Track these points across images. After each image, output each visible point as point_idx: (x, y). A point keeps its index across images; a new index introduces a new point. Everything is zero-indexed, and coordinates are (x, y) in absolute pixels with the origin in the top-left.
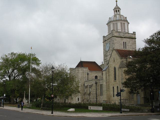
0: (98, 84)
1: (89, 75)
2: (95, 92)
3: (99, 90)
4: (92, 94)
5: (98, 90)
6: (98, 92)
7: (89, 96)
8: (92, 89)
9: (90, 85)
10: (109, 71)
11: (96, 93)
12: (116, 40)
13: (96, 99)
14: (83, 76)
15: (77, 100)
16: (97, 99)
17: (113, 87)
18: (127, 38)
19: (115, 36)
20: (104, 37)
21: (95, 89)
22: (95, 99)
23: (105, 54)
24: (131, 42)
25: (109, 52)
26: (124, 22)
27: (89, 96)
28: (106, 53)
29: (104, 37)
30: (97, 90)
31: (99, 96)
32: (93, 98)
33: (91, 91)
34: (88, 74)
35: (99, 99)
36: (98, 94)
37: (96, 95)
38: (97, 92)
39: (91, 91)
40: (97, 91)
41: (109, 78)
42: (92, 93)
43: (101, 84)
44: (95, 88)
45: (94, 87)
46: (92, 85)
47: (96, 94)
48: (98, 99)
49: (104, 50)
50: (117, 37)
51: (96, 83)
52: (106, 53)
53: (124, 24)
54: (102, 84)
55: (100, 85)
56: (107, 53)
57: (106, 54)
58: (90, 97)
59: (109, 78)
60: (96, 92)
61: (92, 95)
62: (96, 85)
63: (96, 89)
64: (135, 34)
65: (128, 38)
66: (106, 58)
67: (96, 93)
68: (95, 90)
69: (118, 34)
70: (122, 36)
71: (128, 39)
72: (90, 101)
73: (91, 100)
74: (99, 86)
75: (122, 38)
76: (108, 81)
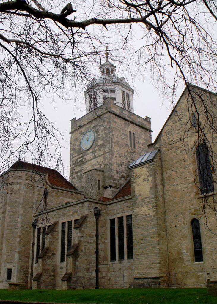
0: (102, 218)
1: (49, 197)
2: (93, 247)
3: (106, 241)
4: (85, 254)
5: (103, 240)
6: (101, 246)
7: (75, 261)
8: (84, 235)
9: (66, 220)
10: (162, 167)
11: (97, 248)
12: (115, 122)
13: (97, 271)
14: (33, 198)
15: (6, 276)
16: (99, 274)
17: (195, 224)
18: (136, 125)
19: (112, 111)
20: (74, 121)
21: (92, 236)
22: (94, 274)
23: (77, 159)
24: (143, 136)
25: (91, 151)
26: (128, 92)
27: (75, 261)
28: (81, 155)
29: (74, 121)
30: (100, 237)
31: (106, 262)
32: (88, 270)
33: (82, 239)
34: (46, 194)
35: (104, 274)
36: (101, 254)
37: (95, 256)
38: (99, 247)
39: (82, 239)
40: (99, 242)
41: (163, 190)
42: (83, 247)
43: (120, 215)
44: (94, 233)
45: (90, 228)
46: (84, 218)
47: (97, 253)
48: (101, 273)
49: (72, 149)
50: (117, 117)
51: (97, 215)
52: (81, 155)
53: (128, 95)
54: (121, 219)
55: (112, 221)
56: (82, 157)
57: (81, 159)
58: (77, 263)
59: (163, 190)
60: (95, 246)
61: (85, 258)
62: (97, 220)
63: (97, 235)
64: (150, 122)
65: (139, 126)
66: (77, 169)
67: (97, 248)
68: (95, 238)
69: (120, 111)
70: (127, 118)
71: (137, 127)
72: (78, 278)
73: (80, 274)
74: (105, 223)
75: (127, 122)
76: (161, 199)
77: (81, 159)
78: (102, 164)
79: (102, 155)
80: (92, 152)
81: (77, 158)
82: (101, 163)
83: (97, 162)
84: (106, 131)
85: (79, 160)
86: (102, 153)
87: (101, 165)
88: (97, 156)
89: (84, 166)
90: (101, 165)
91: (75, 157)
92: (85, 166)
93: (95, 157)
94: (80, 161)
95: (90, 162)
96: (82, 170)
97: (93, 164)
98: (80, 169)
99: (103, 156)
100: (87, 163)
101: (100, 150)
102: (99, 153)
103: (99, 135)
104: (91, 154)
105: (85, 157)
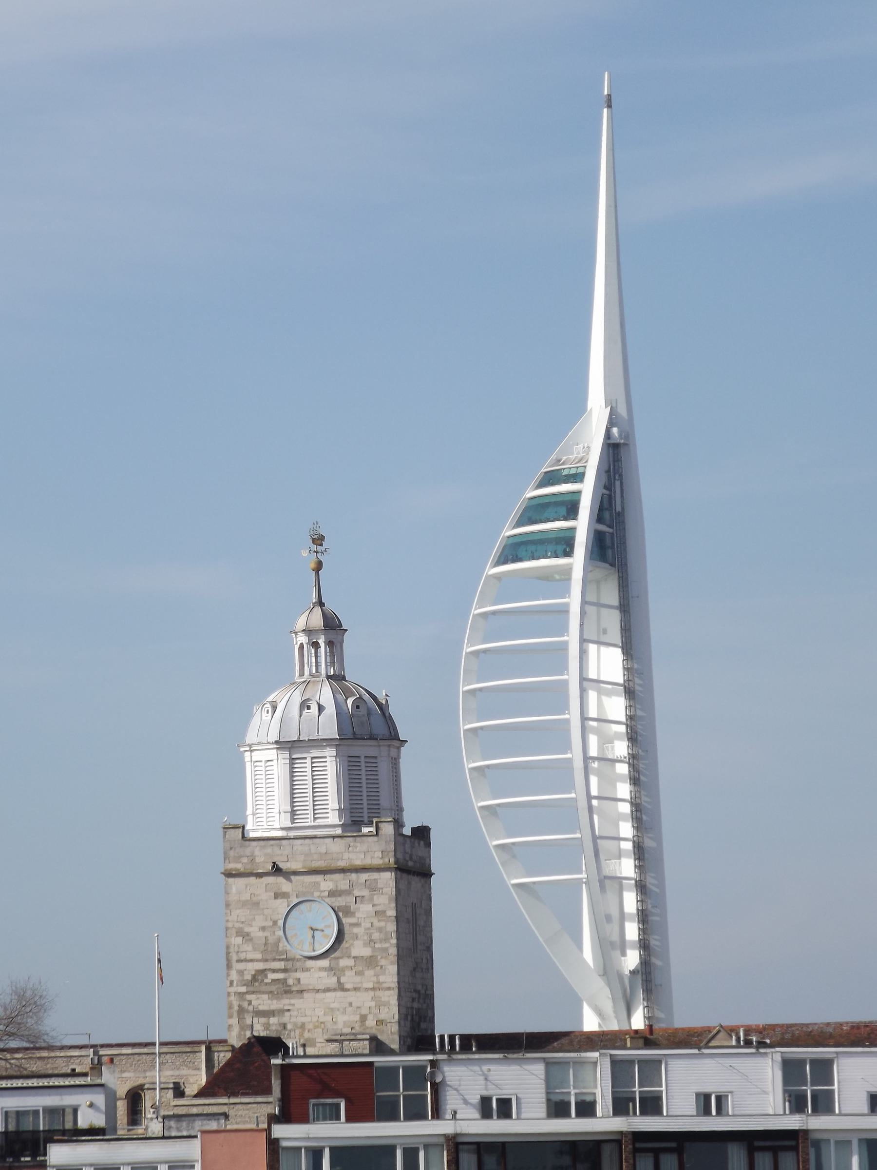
25: (325, 963)
56: (285, 970)
77: (280, 976)
78: (370, 1017)
79: (367, 989)
80: (321, 969)
81: (260, 966)
82: (364, 1011)
83: (351, 1004)
84: (382, 924)
85: (271, 976)
86: (370, 985)
87: (363, 1018)
88: (347, 986)
89: (293, 1001)
90: (363, 1018)
91: (252, 961)
92: (297, 1003)
93: (341, 987)
94: (274, 981)
95: (320, 996)
96: (287, 1014)
97: (333, 1006)
98: (275, 1005)
99: (372, 993)
100: (305, 995)
101: (360, 973)
102: (358, 979)
103: (357, 925)
104: (324, 974)
105: (298, 975)
